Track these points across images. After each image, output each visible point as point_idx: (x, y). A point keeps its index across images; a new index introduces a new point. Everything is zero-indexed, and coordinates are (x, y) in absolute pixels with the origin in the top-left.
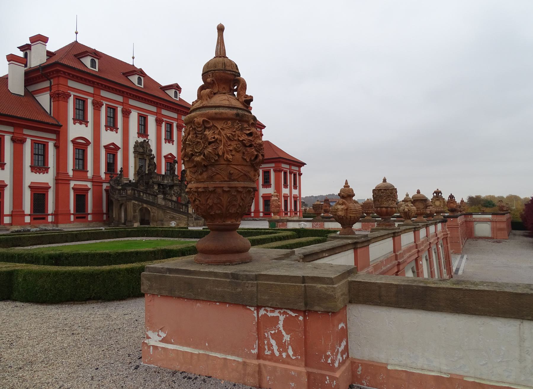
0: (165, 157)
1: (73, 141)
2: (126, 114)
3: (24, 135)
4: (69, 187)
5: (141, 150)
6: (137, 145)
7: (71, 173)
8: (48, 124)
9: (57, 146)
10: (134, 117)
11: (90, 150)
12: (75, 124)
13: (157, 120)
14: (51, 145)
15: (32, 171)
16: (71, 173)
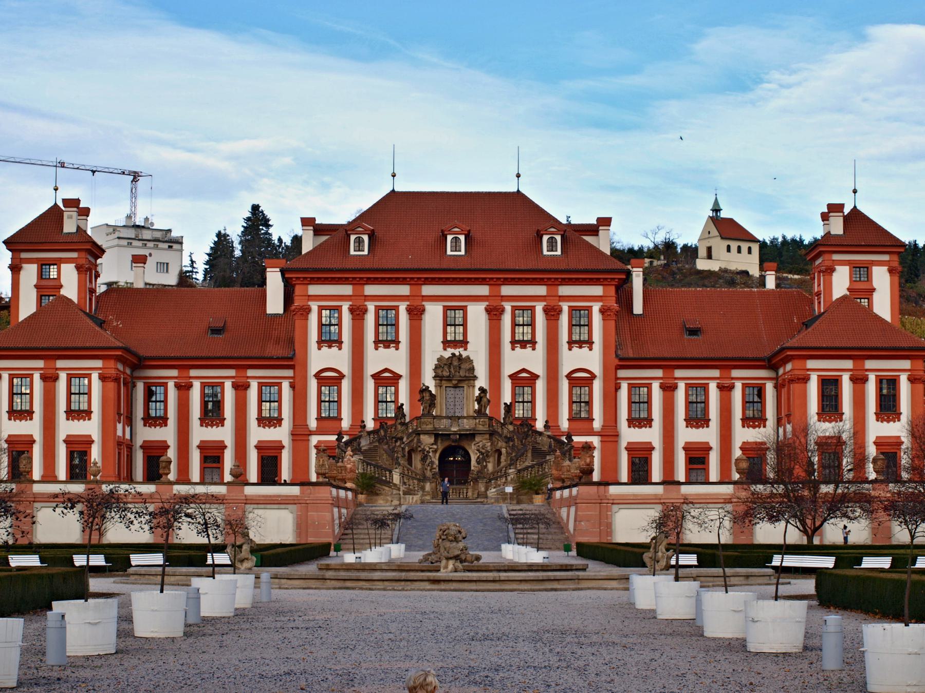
0: (513, 377)
1: (317, 375)
2: (416, 313)
3: (248, 377)
4: (308, 446)
5: (446, 374)
7: (313, 424)
8: (271, 359)
9: (292, 386)
10: (433, 314)
11: (346, 385)
12: (319, 349)
13: (487, 310)
14: (286, 385)
15: (259, 426)
16: (313, 424)
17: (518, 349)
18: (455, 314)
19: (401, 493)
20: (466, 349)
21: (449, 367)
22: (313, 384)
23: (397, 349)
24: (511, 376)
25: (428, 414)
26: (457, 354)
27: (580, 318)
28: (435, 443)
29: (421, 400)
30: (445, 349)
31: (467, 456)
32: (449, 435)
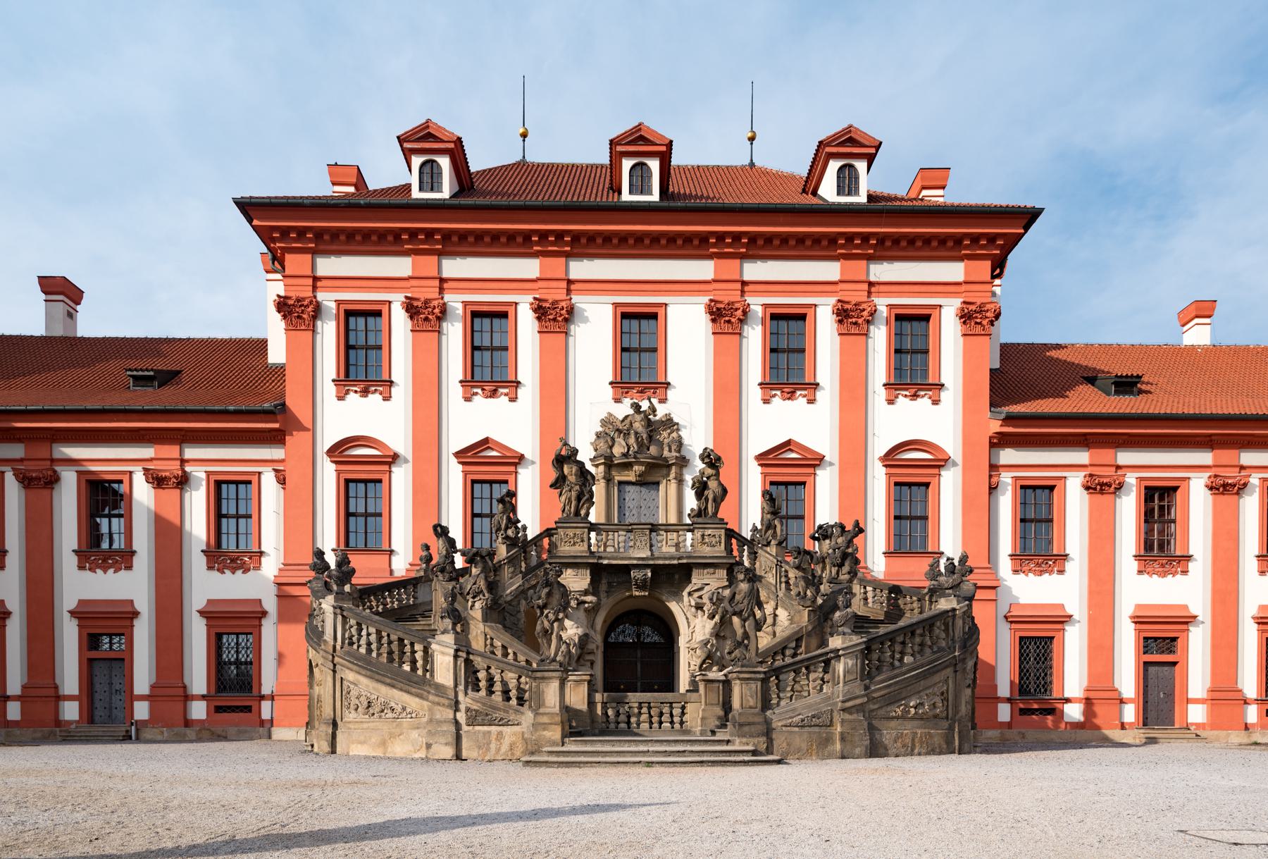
6: (610, 430)
9: (282, 480)
17: (777, 401)
18: (639, 330)
19: (461, 717)
20: (663, 401)
21: (627, 435)
22: (328, 475)
23: (513, 399)
24: (761, 457)
25: (576, 514)
26: (645, 405)
27: (913, 327)
28: (594, 588)
29: (559, 483)
30: (617, 400)
31: (668, 630)
32: (627, 569)
